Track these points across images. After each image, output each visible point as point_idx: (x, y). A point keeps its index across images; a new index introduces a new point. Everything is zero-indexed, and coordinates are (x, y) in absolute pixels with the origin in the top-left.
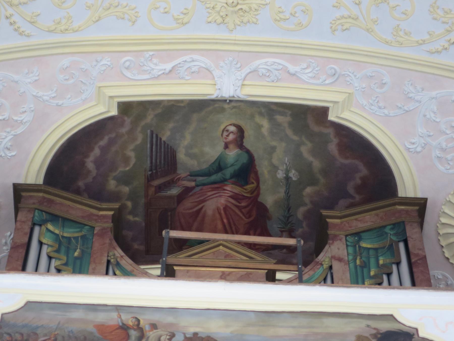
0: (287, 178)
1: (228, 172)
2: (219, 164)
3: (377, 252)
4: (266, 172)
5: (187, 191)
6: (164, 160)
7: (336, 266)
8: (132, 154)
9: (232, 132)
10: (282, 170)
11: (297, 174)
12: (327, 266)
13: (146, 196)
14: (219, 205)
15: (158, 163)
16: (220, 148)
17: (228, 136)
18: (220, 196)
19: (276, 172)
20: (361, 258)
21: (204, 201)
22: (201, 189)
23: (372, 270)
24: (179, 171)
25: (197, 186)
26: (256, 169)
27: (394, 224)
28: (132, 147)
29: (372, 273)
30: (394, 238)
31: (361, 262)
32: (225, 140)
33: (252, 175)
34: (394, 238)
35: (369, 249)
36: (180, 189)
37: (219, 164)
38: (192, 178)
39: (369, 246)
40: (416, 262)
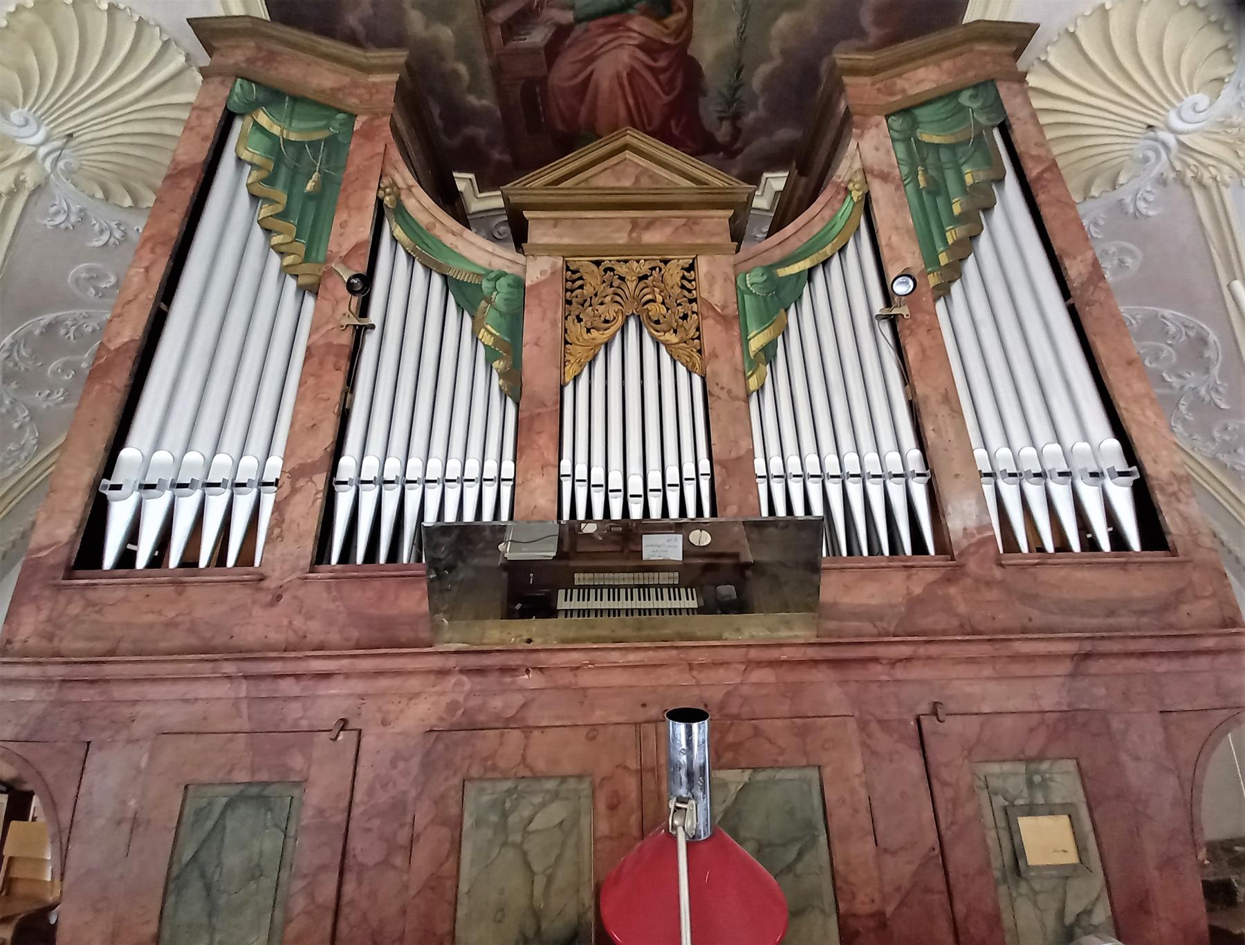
3: (955, 155)
7: (878, 191)
12: (860, 193)
13: (489, 50)
14: (620, 68)
18: (621, 46)
20: (925, 171)
21: (591, 59)
22: (587, 30)
23: (954, 201)
27: (975, 87)
29: (957, 209)
30: (982, 120)
31: (926, 180)
34: (982, 120)
35: (938, 146)
36: (546, 30)
39: (936, 140)
40: (1039, 177)
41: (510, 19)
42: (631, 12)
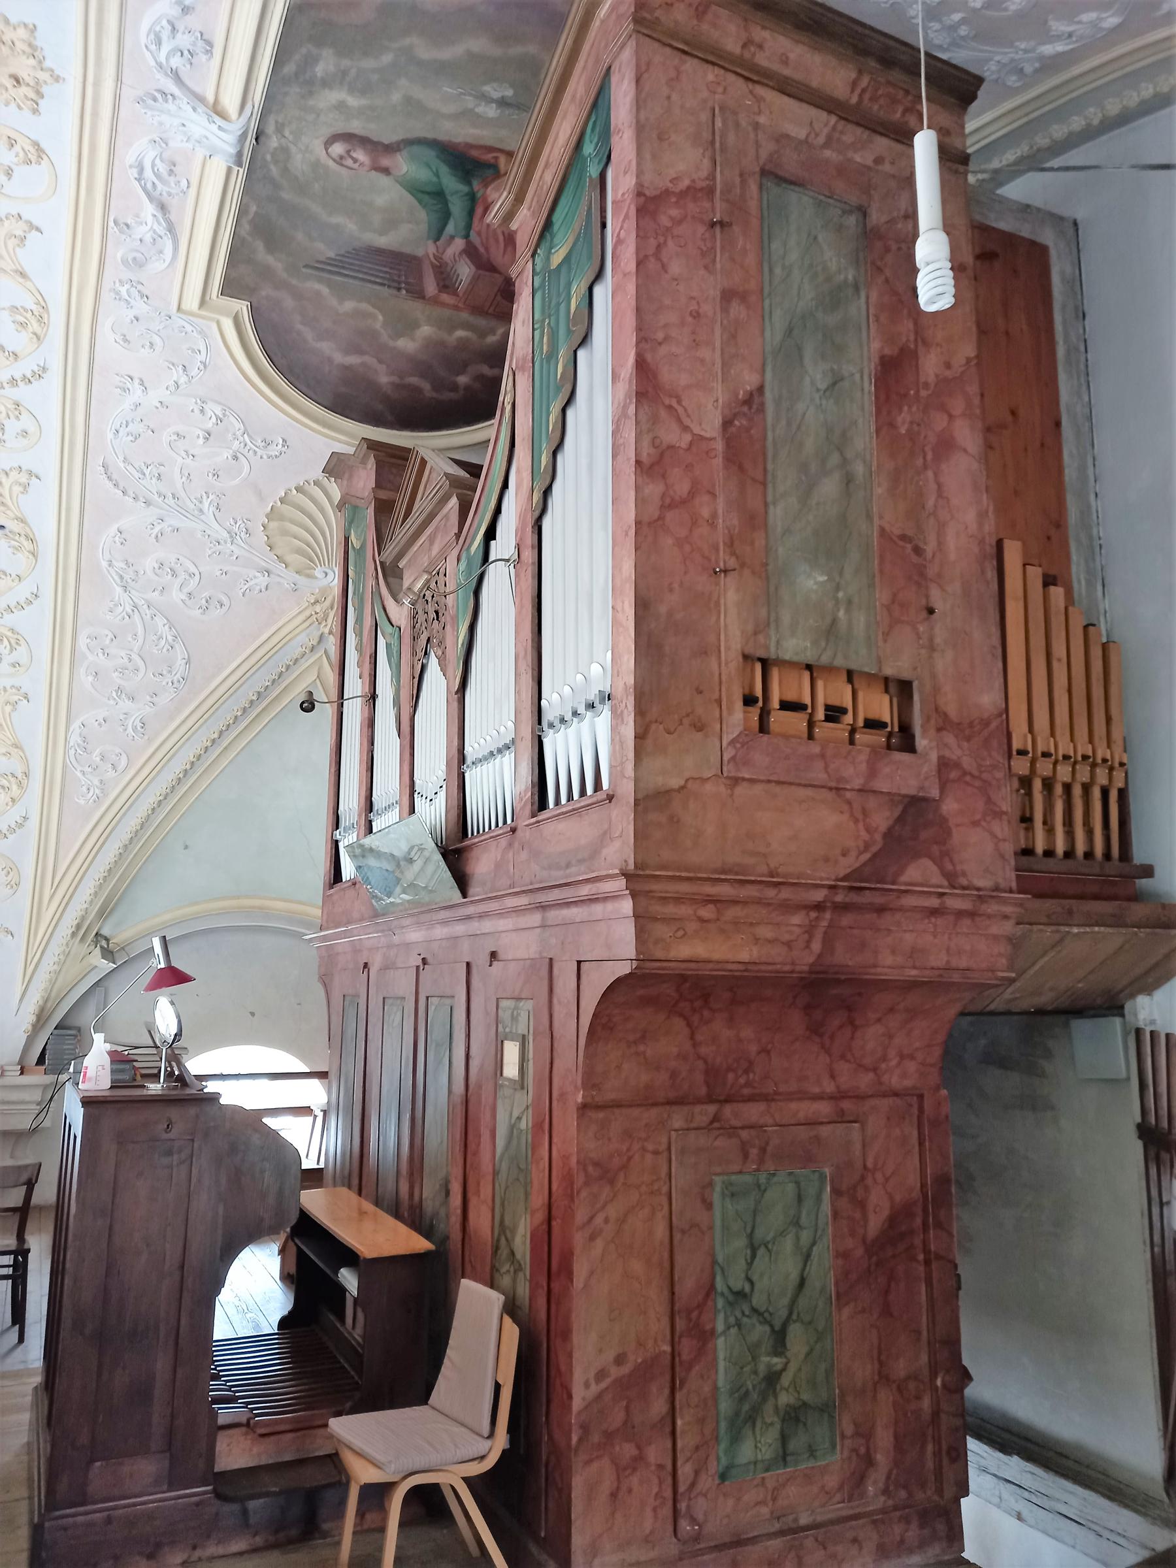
0: (502, 103)
1: (451, 183)
2: (428, 193)
4: (472, 131)
5: (471, 252)
6: (385, 266)
8: (349, 305)
9: (348, 152)
10: (479, 105)
11: (495, 85)
15: (388, 276)
16: (383, 180)
17: (355, 161)
19: (478, 116)
22: (479, 234)
24: (420, 252)
25: (467, 236)
26: (460, 144)
28: (334, 302)
32: (366, 168)
33: (475, 153)
36: (462, 262)
37: (428, 193)
38: (443, 239)
41: (438, 285)
42: (479, 195)
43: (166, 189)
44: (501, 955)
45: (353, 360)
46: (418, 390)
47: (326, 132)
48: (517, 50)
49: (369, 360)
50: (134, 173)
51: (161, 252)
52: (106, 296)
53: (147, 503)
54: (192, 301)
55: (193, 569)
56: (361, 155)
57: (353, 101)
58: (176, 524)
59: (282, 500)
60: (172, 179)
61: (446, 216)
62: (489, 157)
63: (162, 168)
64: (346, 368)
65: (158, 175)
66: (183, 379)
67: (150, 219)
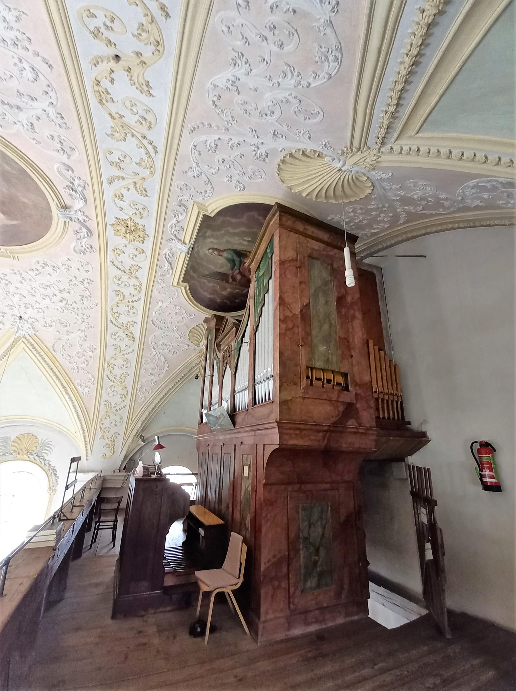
1: (236, 258)
5: (240, 273)
8: (211, 284)
25: (239, 269)
28: (208, 284)
38: (234, 270)
43: (171, 259)
44: (244, 443)
45: (211, 296)
46: (227, 303)
47: (209, 247)
48: (252, 230)
49: (216, 296)
50: (164, 256)
51: (169, 273)
52: (156, 282)
53: (161, 329)
54: (175, 284)
55: (171, 345)
56: (216, 252)
57: (214, 241)
58: (167, 334)
59: (193, 328)
60: (173, 258)
61: (234, 265)
62: (244, 252)
63: (171, 255)
64: (210, 298)
65: (170, 257)
66: (172, 301)
67: (167, 266)
